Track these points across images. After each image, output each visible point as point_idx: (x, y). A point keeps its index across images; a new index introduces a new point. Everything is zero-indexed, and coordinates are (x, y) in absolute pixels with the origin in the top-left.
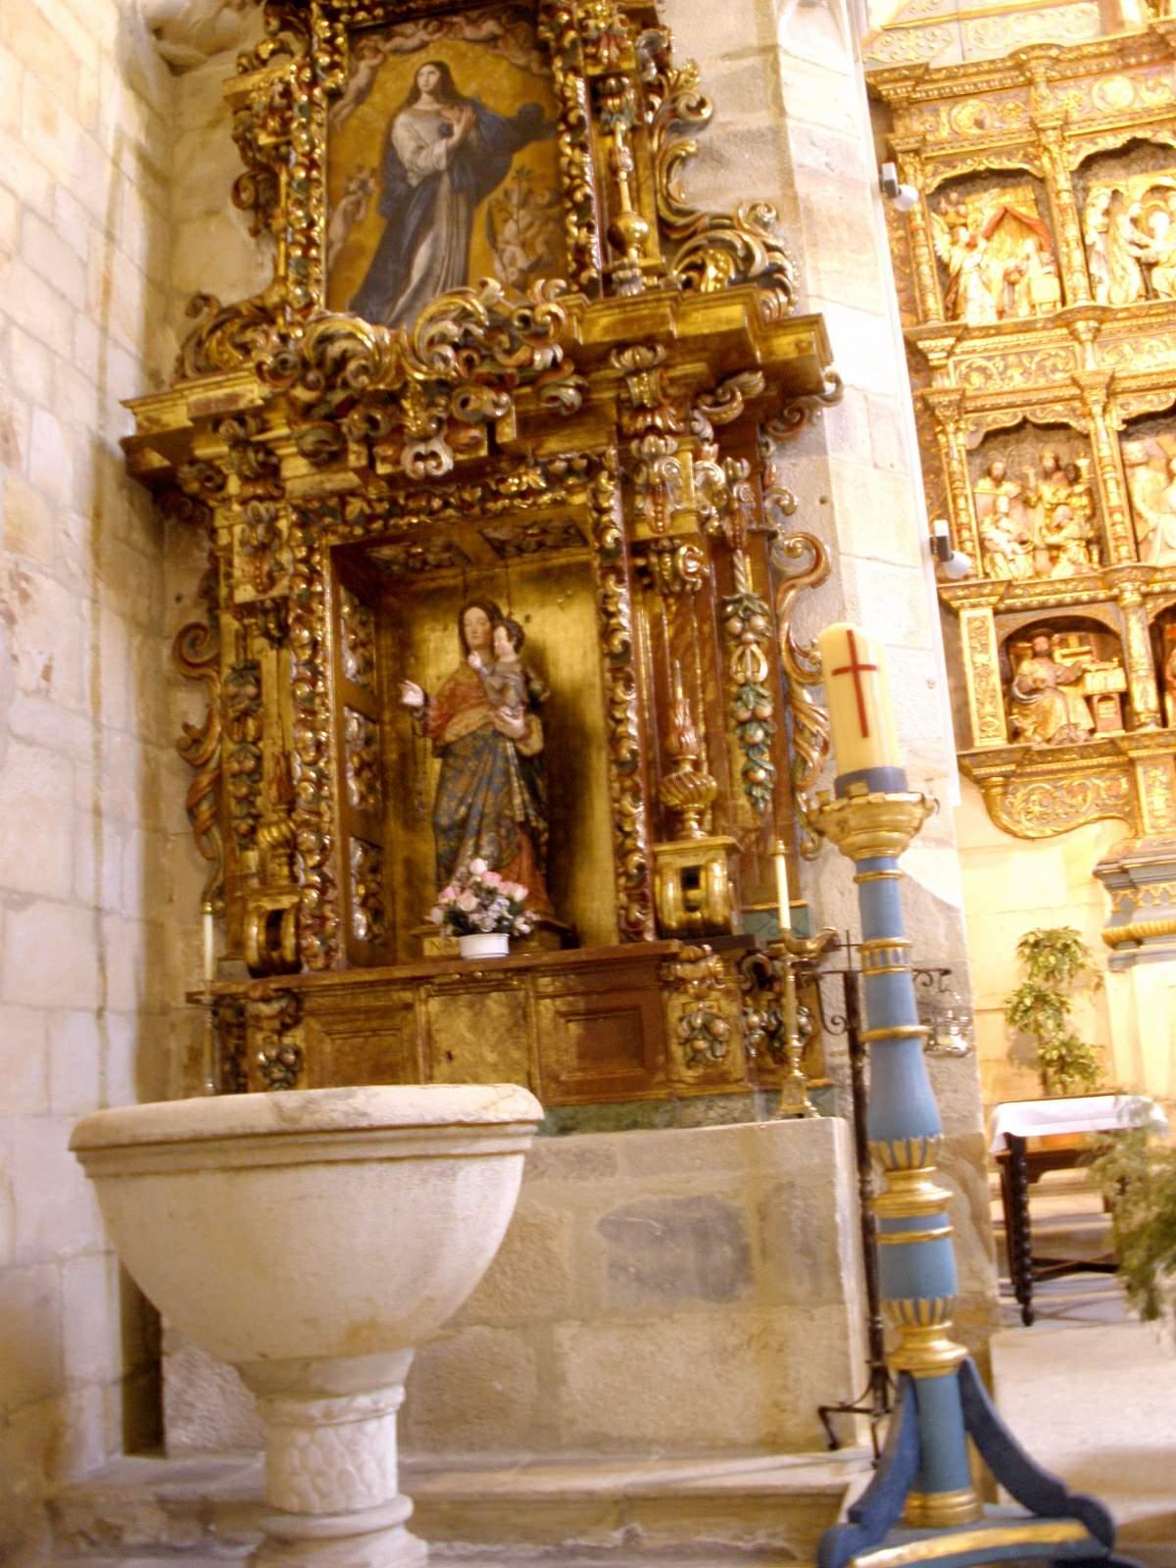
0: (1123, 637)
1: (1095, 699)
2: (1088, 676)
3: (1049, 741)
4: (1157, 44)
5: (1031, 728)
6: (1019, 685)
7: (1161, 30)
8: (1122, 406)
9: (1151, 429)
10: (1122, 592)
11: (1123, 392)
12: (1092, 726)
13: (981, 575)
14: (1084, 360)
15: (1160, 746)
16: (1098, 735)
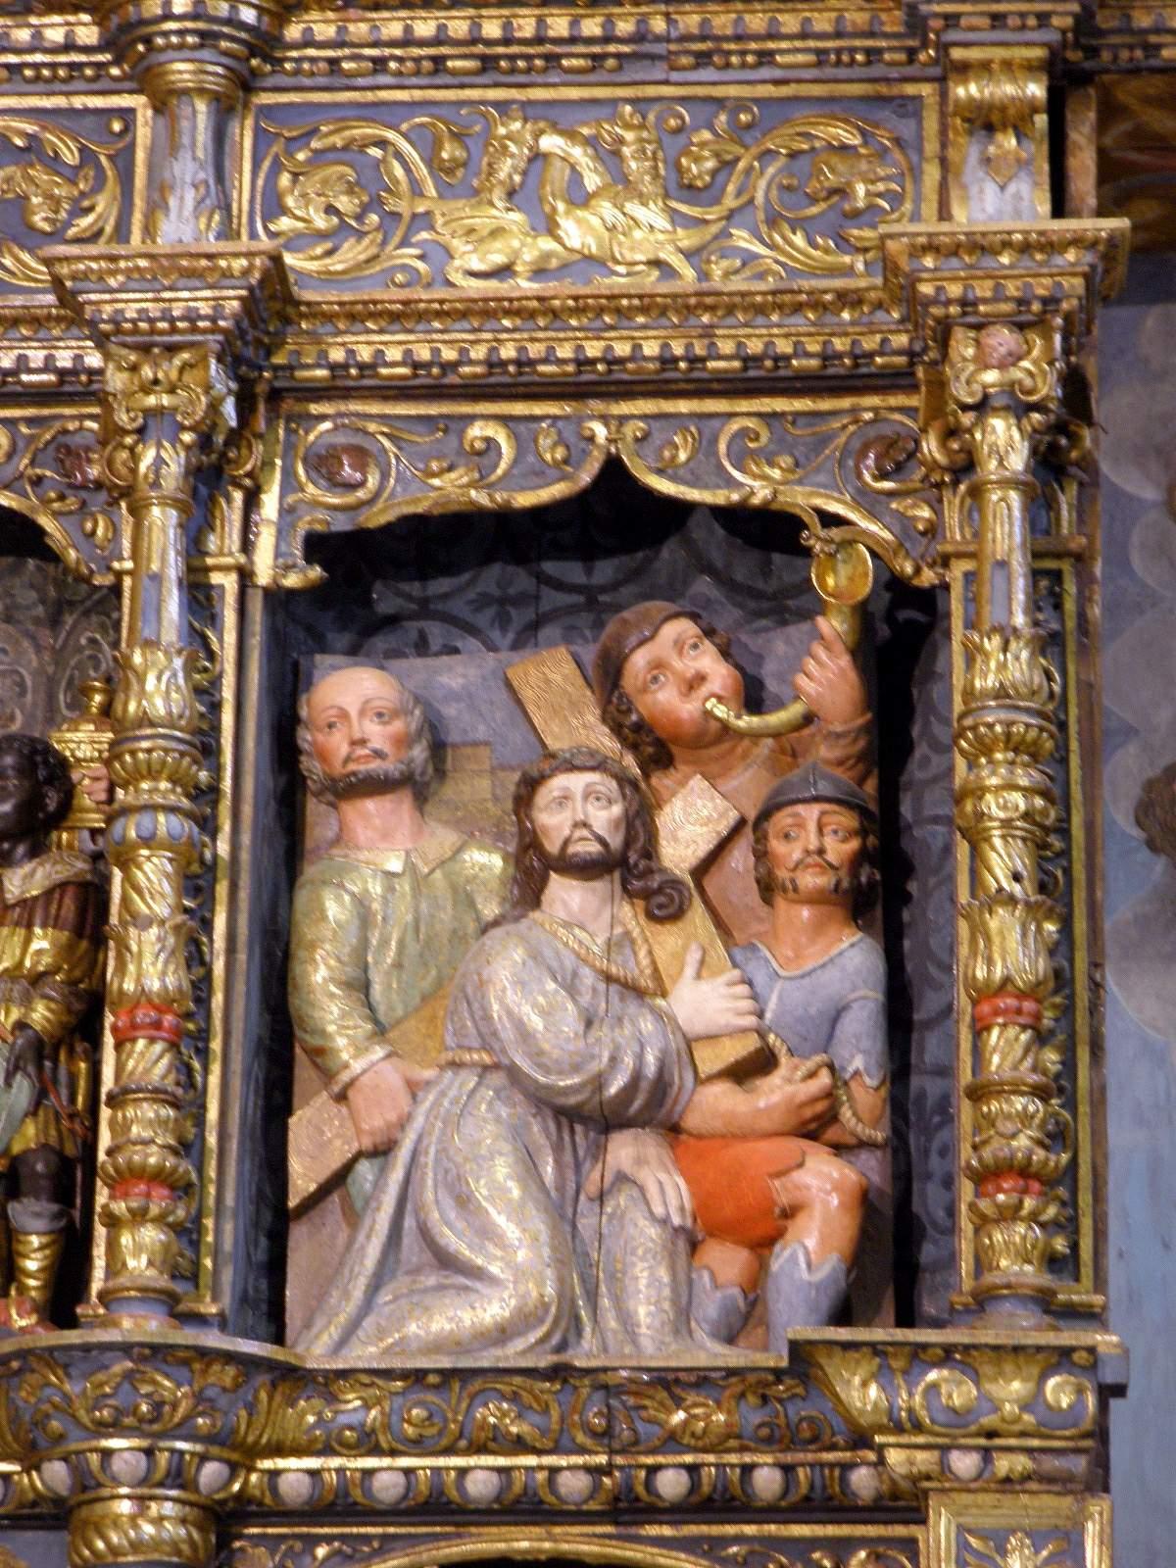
8: (324, 464)
9: (503, 604)
10: (89, 1486)
11: (337, 388)
14: (160, 194)
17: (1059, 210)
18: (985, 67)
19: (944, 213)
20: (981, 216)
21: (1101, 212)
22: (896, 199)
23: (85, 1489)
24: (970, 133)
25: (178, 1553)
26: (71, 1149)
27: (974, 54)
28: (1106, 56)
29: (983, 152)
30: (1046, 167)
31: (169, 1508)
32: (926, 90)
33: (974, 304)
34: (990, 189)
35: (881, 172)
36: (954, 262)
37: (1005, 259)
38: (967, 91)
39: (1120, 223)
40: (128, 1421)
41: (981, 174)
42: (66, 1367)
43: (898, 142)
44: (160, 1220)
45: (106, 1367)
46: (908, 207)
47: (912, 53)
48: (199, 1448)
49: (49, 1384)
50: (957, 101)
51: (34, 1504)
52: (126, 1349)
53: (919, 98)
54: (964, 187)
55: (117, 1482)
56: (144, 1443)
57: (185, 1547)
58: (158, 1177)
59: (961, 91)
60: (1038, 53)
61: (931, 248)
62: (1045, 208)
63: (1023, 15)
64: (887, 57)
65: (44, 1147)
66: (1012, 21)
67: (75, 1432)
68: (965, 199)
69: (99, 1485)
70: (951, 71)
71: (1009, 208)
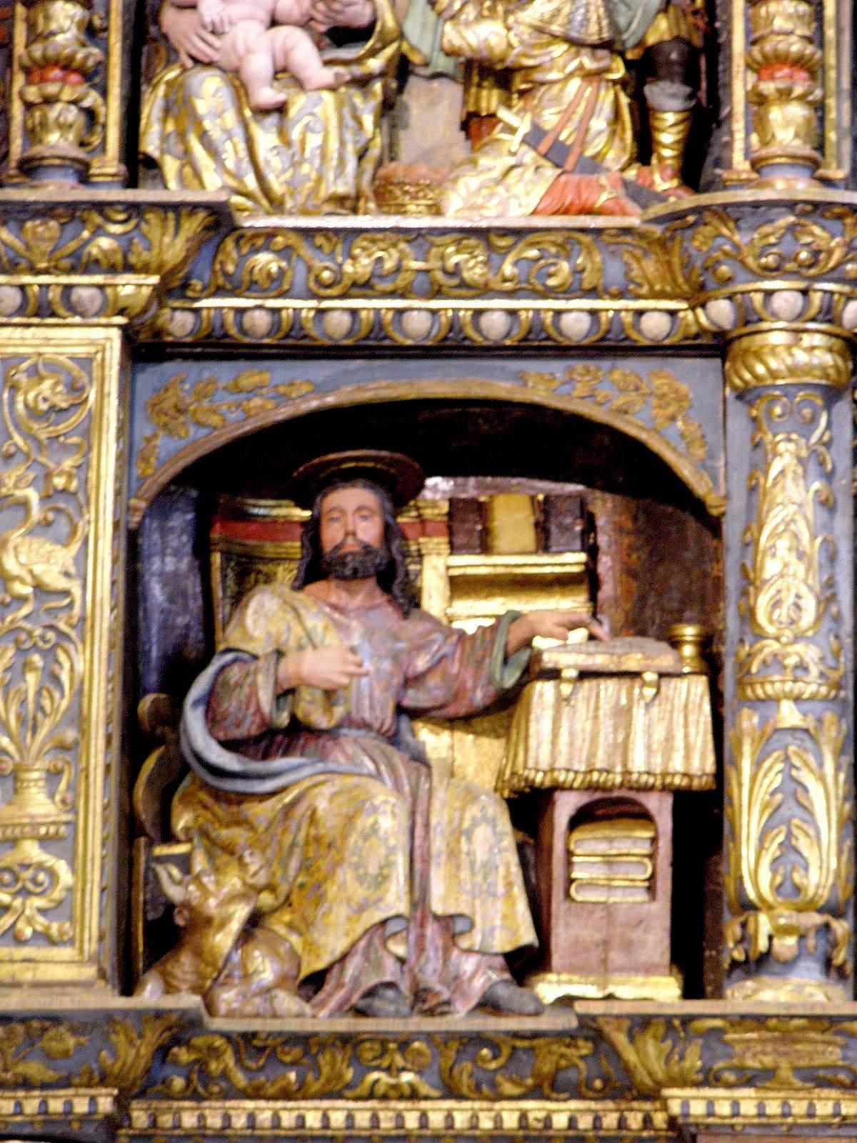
0: (732, 530)
1: (565, 807)
2: (543, 691)
3: (314, 983)
5: (241, 913)
6: (209, 701)
10: (749, 319)
12: (528, 936)
13: (110, 163)
15: (818, 1079)
16: (548, 988)
23: (747, 323)
25: (827, 376)
26: (698, 41)
31: (818, 340)
40: (790, 266)
42: (737, 220)
44: (801, 98)
45: (771, 221)
48: (846, 289)
49: (720, 235)
51: (697, 336)
52: (790, 205)
55: (775, 316)
56: (802, 285)
57: (832, 372)
58: (799, 62)
65: (677, 39)
67: (742, 275)
69: (761, 320)
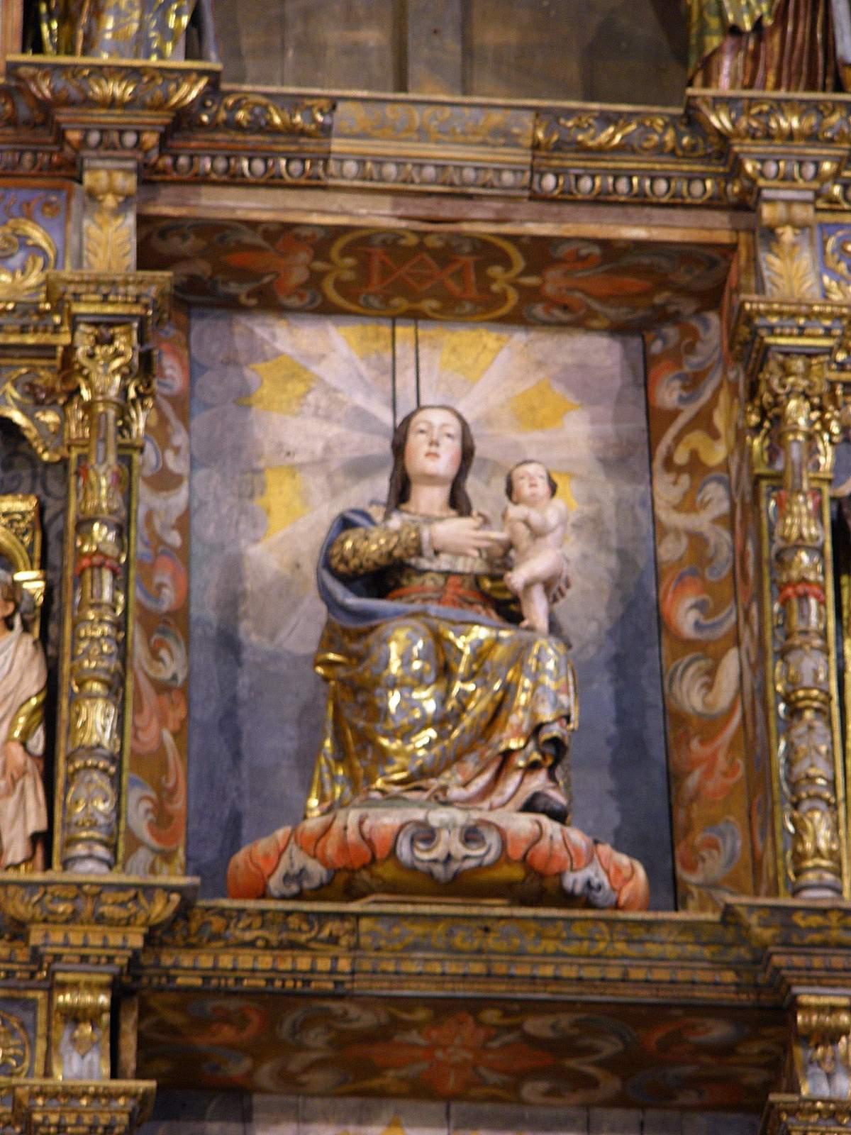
4: (31, 125)
7: (45, 89)
17: (114, 1074)
18: (74, 986)
19: (48, 1073)
20: (69, 1074)
21: (140, 1075)
22: (20, 1060)
24: (65, 1022)
27: (70, 977)
28: (145, 981)
29: (72, 1034)
30: (108, 1045)
32: (40, 995)
33: (65, 1127)
34: (76, 1058)
35: (12, 1042)
36: (55, 1102)
37: (84, 1102)
38: (65, 998)
39: (150, 1084)
41: (70, 1048)
43: (22, 1025)
46: (26, 1064)
47: (33, 974)
50: (58, 1005)
53: (34, 1001)
54: (61, 1056)
59: (61, 999)
60: (106, 979)
61: (42, 1093)
62: (106, 1070)
63: (99, 957)
64: (18, 975)
66: (92, 960)
68: (61, 1062)
70: (53, 987)
71: (86, 1069)
